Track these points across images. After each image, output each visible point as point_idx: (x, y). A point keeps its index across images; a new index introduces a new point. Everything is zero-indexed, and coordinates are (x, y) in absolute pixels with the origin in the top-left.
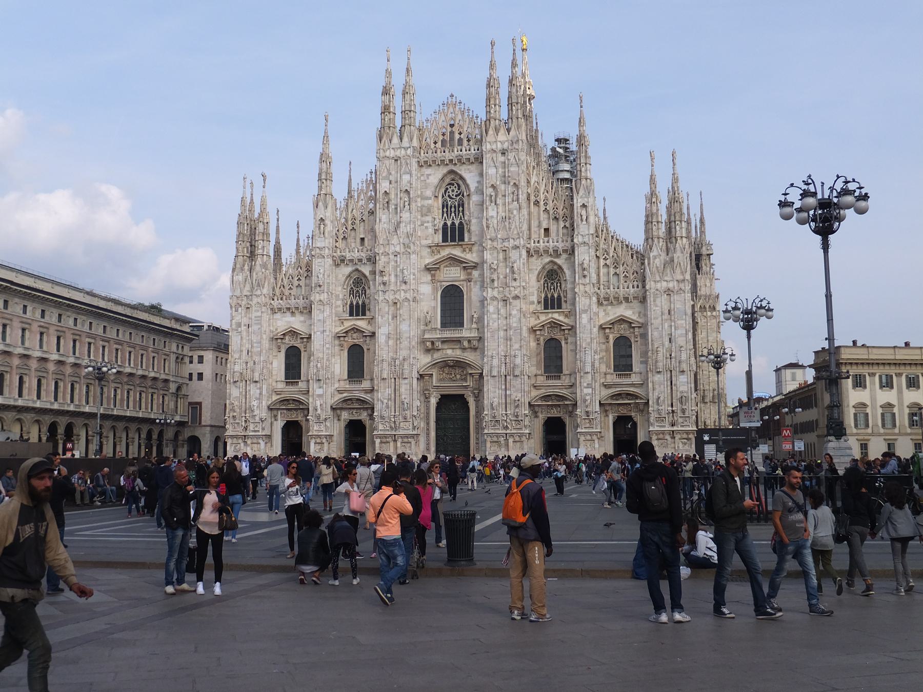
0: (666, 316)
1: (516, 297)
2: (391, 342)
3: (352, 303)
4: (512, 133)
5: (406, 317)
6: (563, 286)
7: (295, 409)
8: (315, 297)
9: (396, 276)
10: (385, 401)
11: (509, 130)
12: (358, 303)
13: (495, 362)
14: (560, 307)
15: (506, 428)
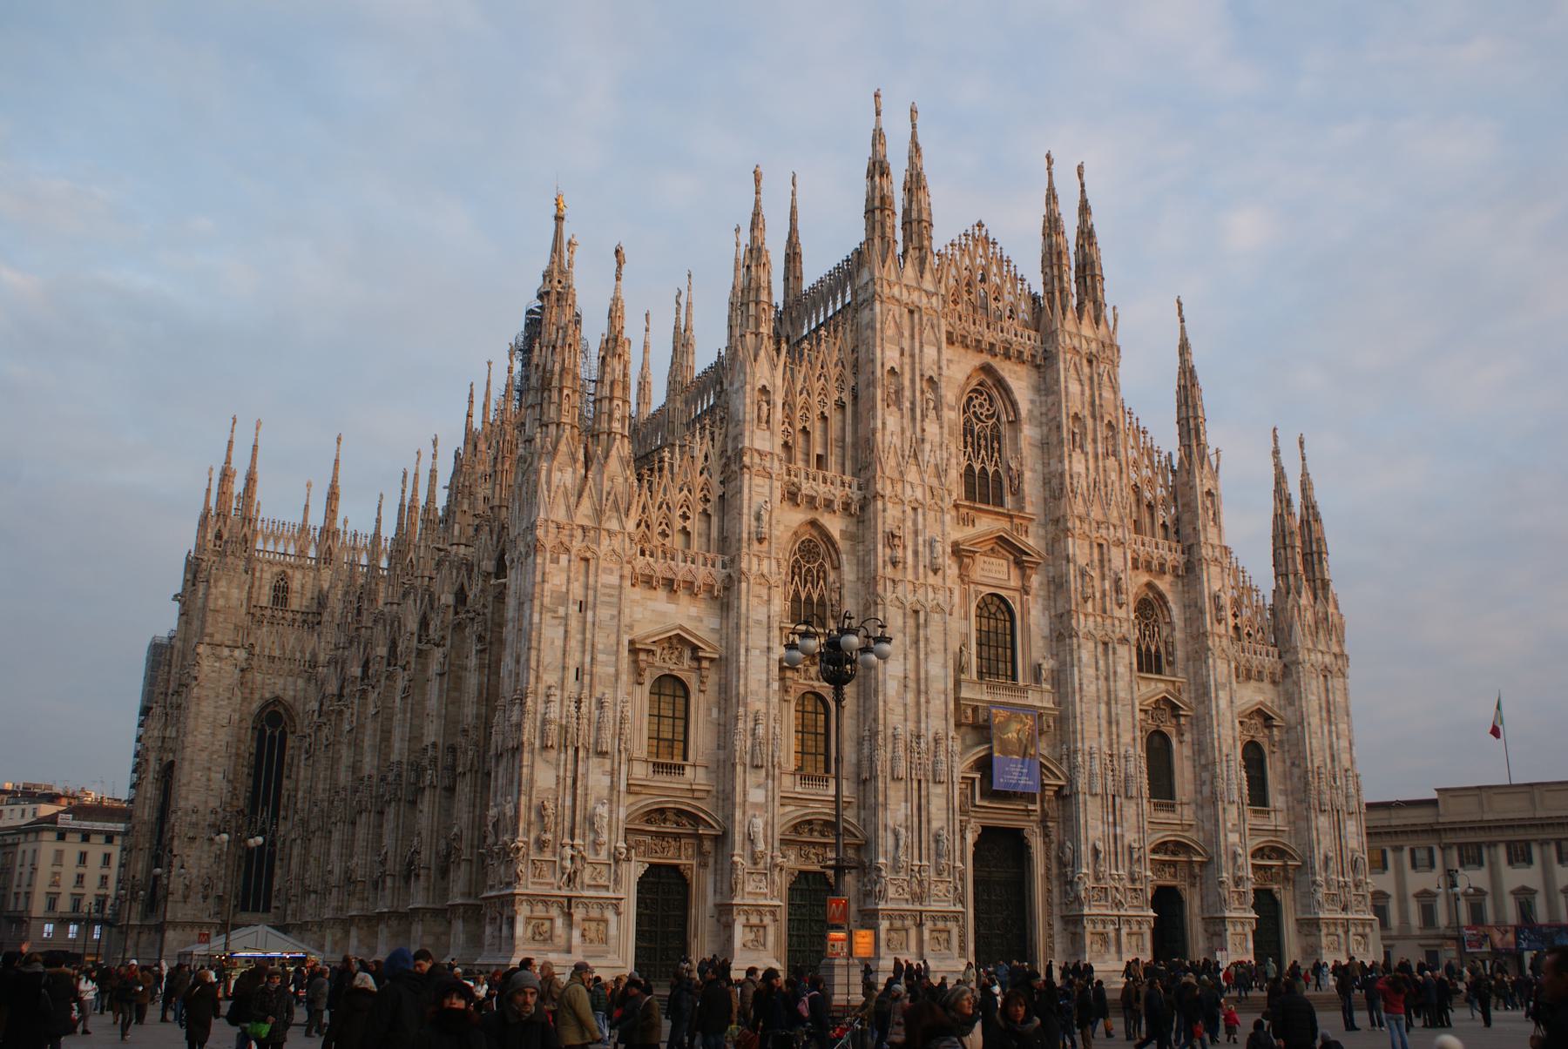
0: (1324, 714)
1: (1124, 640)
2: (910, 697)
3: (797, 593)
4: (1102, 327)
5: (936, 644)
6: (1165, 631)
7: (677, 837)
8: (749, 563)
9: (916, 553)
10: (903, 831)
11: (1097, 323)
12: (809, 597)
13: (1097, 768)
14: (1159, 671)
15: (1118, 905)
